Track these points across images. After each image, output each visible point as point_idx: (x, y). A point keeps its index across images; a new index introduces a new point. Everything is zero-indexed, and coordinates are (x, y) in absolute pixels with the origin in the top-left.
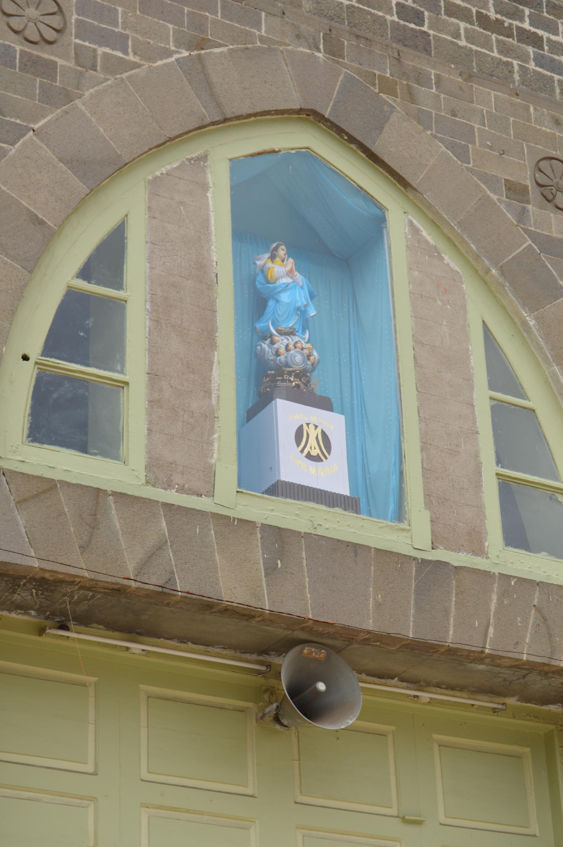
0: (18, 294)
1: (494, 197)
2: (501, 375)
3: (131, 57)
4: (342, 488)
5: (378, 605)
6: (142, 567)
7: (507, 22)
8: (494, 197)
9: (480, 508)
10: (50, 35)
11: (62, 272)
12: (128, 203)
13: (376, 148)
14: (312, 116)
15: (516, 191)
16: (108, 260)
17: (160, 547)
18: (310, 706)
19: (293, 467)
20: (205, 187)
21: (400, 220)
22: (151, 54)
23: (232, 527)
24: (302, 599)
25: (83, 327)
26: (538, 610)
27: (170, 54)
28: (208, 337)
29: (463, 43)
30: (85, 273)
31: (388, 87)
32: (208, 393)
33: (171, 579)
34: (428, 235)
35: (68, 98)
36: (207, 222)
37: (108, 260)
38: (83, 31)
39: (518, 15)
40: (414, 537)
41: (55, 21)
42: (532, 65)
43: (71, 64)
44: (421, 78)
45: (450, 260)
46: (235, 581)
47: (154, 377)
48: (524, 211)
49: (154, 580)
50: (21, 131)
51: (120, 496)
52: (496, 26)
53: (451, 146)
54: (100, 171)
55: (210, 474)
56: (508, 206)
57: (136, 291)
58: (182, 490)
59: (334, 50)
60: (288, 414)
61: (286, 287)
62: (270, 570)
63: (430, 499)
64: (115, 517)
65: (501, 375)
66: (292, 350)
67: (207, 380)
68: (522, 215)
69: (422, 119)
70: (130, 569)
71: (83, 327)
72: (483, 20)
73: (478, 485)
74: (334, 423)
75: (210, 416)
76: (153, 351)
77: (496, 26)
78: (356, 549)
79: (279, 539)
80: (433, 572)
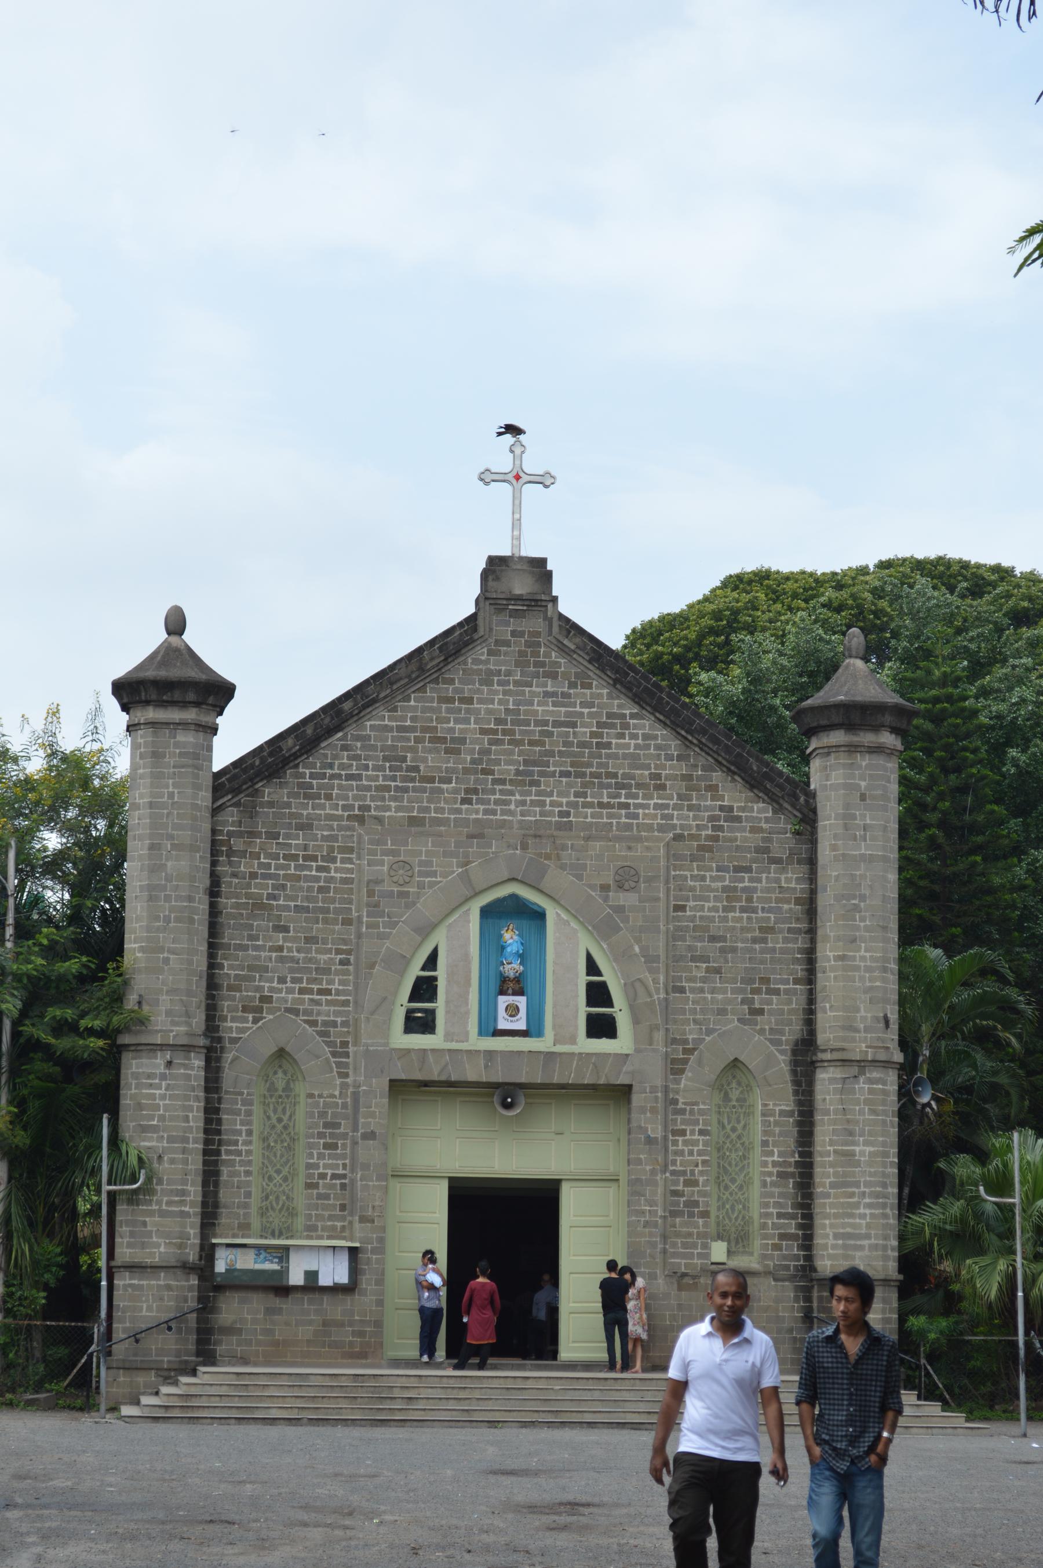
0: (399, 984)
1: (593, 894)
2: (592, 968)
3: (439, 879)
4: (524, 1028)
5: (527, 1072)
6: (439, 1075)
7: (612, 801)
8: (593, 894)
9: (576, 1027)
10: (407, 879)
11: (415, 971)
12: (440, 938)
13: (541, 887)
14: (513, 879)
15: (605, 888)
16: (432, 962)
17: (446, 1065)
18: (508, 1106)
19: (503, 1024)
20: (469, 922)
21: (552, 913)
22: (445, 875)
23: (471, 1053)
24: (499, 1077)
25: (424, 989)
26: (594, 1064)
27: (453, 872)
28: (468, 982)
29: (589, 820)
30: (423, 969)
31: (548, 857)
32: (467, 1004)
33: (450, 1076)
34: (564, 916)
35: (414, 904)
36: (469, 938)
37: (432, 962)
38: (421, 874)
39: (618, 796)
40: (543, 1044)
41: (410, 873)
42: (624, 820)
43: (416, 890)
44: (564, 848)
45: (574, 924)
46: (473, 1073)
47: (447, 1002)
48: (608, 896)
49: (443, 1078)
50: (397, 923)
51: (433, 1050)
52: (608, 806)
53: (574, 876)
54: (426, 930)
55: (467, 1034)
56: (600, 896)
57: (441, 973)
58: (457, 1041)
59: (524, 847)
60: (503, 1001)
61: (510, 945)
62: (486, 1066)
63: (554, 1027)
64: (431, 1057)
65: (592, 968)
66: (512, 968)
67: (467, 999)
68: (606, 899)
69: (563, 867)
70: (436, 1073)
71: (424, 989)
72: (601, 805)
73: (576, 1017)
74: (521, 1001)
75: (467, 1013)
76: (447, 993)
77: (608, 806)
78: (520, 1053)
79: (490, 1054)
80: (550, 1057)
